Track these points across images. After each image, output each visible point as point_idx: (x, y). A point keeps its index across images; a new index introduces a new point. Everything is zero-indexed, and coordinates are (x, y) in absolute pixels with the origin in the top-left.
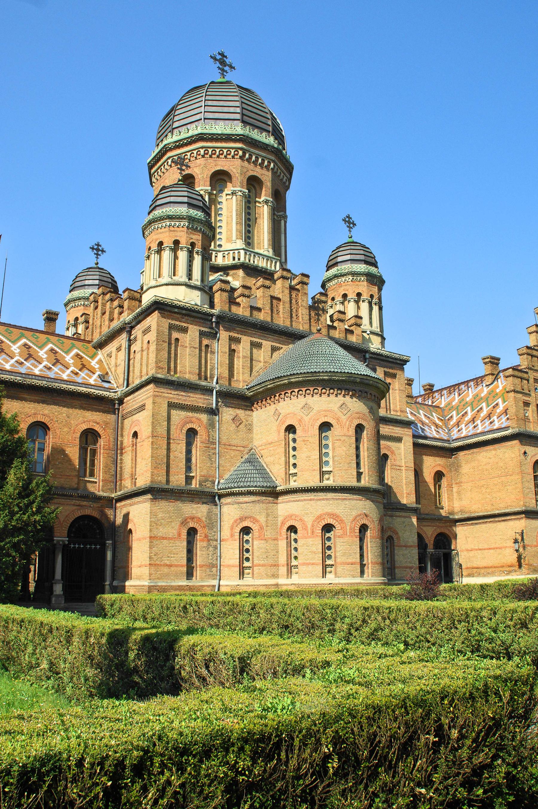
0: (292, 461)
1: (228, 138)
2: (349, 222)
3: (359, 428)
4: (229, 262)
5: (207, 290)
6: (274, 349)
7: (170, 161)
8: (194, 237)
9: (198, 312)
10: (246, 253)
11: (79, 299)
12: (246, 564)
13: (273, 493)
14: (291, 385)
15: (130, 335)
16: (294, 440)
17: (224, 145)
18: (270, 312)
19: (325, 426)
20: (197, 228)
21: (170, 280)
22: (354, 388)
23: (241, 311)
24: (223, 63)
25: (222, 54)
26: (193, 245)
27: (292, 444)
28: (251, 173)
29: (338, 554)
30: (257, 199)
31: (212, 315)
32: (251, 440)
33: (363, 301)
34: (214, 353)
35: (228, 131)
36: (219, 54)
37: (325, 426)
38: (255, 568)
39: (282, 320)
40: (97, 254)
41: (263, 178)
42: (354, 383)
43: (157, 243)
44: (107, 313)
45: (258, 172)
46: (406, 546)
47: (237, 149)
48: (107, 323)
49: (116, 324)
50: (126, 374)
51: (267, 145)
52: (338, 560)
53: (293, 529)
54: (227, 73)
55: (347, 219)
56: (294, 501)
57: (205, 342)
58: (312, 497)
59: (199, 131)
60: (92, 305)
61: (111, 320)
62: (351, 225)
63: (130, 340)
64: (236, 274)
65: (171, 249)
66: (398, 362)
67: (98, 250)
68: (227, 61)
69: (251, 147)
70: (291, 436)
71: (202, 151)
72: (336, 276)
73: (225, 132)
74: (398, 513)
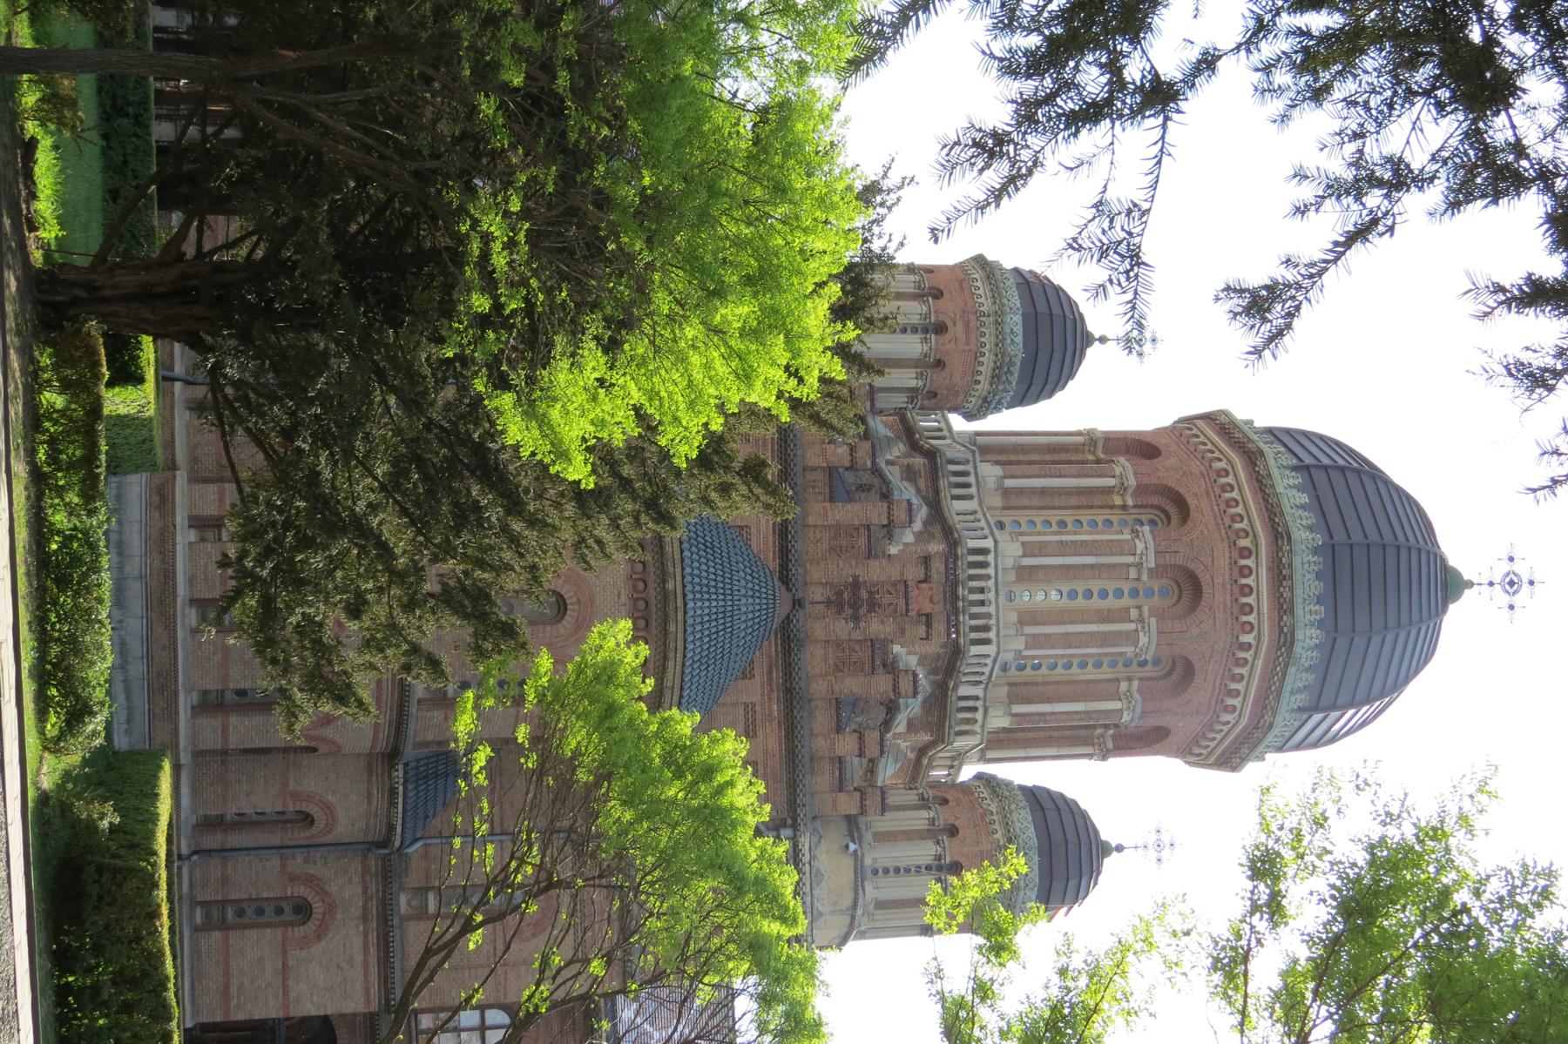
1: (1272, 512)
4: (957, 521)
8: (960, 328)
10: (984, 551)
20: (983, 335)
22: (652, 585)
24: (1512, 584)
26: (940, 329)
28: (1205, 579)
33: (938, 843)
45: (1217, 595)
46: (285, 970)
51: (1292, 611)
64: (932, 536)
69: (1269, 569)
73: (1286, 505)
74: (373, 938)
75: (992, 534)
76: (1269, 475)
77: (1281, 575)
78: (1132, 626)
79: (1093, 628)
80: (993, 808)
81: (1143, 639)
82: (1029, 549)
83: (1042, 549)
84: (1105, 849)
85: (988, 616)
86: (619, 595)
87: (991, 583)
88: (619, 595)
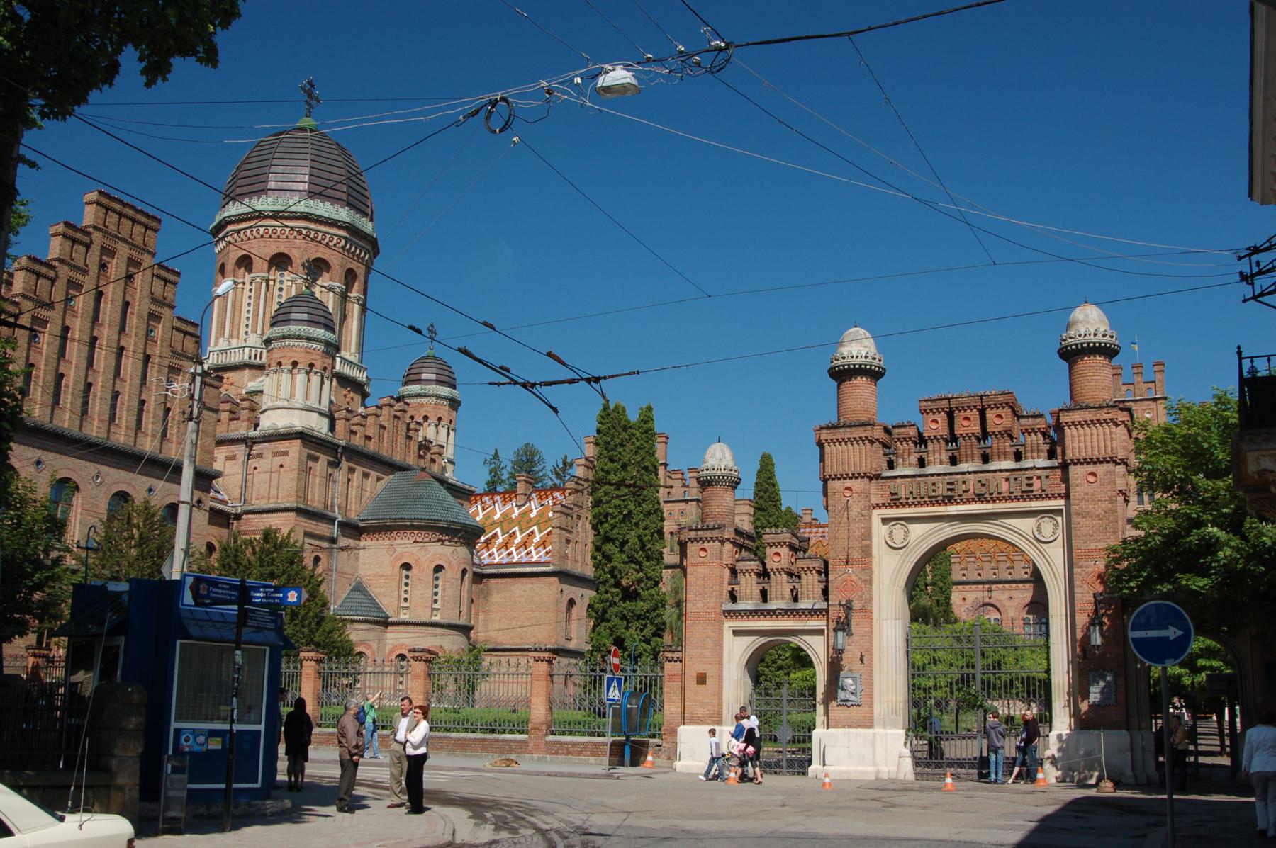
0: (404, 596)
1: (334, 223)
3: (464, 572)
6: (379, 479)
13: (385, 623)
14: (412, 527)
16: (407, 577)
17: (327, 229)
19: (439, 568)
23: (357, 441)
25: (312, 86)
27: (405, 580)
32: (356, 569)
37: (439, 568)
39: (385, 452)
47: (340, 237)
57: (330, 471)
70: (405, 572)
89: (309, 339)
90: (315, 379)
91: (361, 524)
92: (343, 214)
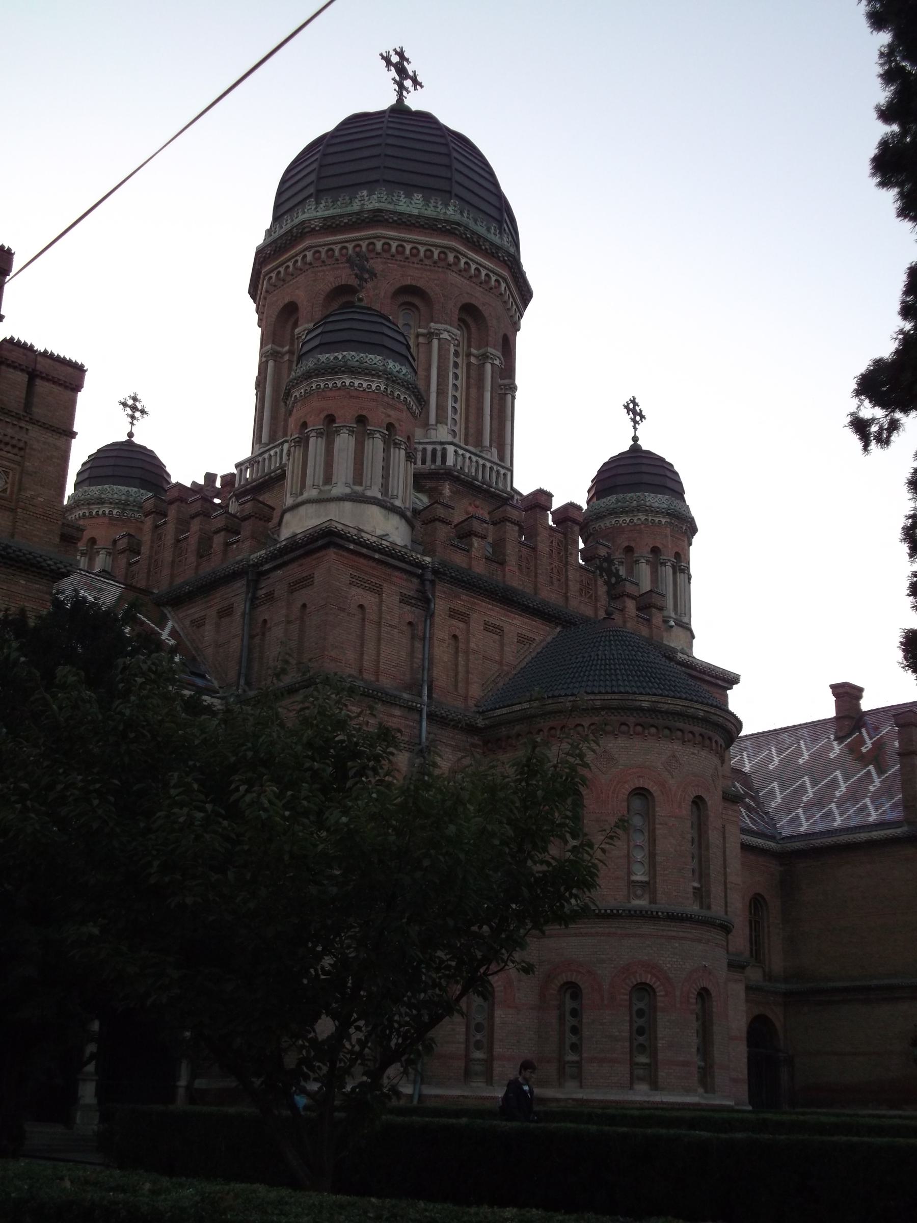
2: (635, 413)
5: (412, 518)
7: (309, 256)
8: (392, 413)
9: (402, 559)
10: (455, 451)
11: (101, 502)
12: (478, 1055)
15: (256, 589)
18: (516, 569)
21: (348, 491)
22: (692, 728)
24: (401, 71)
28: (466, 300)
29: (660, 1044)
30: (473, 351)
31: (423, 567)
33: (663, 564)
34: (424, 638)
35: (430, 212)
36: (397, 53)
38: (496, 1064)
40: (133, 417)
41: (486, 311)
42: (694, 718)
43: (322, 416)
44: (193, 541)
45: (479, 297)
47: (444, 251)
48: (192, 559)
49: (214, 564)
50: (244, 664)
51: (498, 248)
52: (661, 1056)
53: (573, 990)
54: (408, 92)
55: (631, 406)
56: (576, 935)
58: (613, 930)
59: (373, 204)
60: (149, 521)
61: (204, 551)
62: (638, 418)
63: (254, 599)
65: (351, 432)
66: (720, 683)
67: (134, 408)
68: (410, 68)
71: (379, 245)
72: (613, 512)
75: (442, 443)
76: (401, 214)
77: (475, 243)
78: (488, 367)
79: (488, 396)
80: (643, 518)
81: (497, 362)
82: (441, 419)
83: (441, 408)
84: (635, 448)
85: (491, 468)
86: (693, 754)
87: (474, 458)
88: (693, 754)
89: (353, 371)
90: (375, 447)
91: (480, 722)
92: (451, 212)
